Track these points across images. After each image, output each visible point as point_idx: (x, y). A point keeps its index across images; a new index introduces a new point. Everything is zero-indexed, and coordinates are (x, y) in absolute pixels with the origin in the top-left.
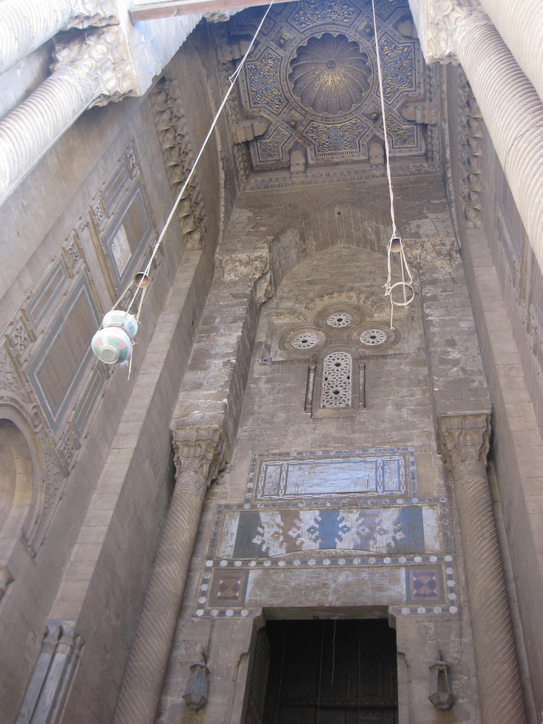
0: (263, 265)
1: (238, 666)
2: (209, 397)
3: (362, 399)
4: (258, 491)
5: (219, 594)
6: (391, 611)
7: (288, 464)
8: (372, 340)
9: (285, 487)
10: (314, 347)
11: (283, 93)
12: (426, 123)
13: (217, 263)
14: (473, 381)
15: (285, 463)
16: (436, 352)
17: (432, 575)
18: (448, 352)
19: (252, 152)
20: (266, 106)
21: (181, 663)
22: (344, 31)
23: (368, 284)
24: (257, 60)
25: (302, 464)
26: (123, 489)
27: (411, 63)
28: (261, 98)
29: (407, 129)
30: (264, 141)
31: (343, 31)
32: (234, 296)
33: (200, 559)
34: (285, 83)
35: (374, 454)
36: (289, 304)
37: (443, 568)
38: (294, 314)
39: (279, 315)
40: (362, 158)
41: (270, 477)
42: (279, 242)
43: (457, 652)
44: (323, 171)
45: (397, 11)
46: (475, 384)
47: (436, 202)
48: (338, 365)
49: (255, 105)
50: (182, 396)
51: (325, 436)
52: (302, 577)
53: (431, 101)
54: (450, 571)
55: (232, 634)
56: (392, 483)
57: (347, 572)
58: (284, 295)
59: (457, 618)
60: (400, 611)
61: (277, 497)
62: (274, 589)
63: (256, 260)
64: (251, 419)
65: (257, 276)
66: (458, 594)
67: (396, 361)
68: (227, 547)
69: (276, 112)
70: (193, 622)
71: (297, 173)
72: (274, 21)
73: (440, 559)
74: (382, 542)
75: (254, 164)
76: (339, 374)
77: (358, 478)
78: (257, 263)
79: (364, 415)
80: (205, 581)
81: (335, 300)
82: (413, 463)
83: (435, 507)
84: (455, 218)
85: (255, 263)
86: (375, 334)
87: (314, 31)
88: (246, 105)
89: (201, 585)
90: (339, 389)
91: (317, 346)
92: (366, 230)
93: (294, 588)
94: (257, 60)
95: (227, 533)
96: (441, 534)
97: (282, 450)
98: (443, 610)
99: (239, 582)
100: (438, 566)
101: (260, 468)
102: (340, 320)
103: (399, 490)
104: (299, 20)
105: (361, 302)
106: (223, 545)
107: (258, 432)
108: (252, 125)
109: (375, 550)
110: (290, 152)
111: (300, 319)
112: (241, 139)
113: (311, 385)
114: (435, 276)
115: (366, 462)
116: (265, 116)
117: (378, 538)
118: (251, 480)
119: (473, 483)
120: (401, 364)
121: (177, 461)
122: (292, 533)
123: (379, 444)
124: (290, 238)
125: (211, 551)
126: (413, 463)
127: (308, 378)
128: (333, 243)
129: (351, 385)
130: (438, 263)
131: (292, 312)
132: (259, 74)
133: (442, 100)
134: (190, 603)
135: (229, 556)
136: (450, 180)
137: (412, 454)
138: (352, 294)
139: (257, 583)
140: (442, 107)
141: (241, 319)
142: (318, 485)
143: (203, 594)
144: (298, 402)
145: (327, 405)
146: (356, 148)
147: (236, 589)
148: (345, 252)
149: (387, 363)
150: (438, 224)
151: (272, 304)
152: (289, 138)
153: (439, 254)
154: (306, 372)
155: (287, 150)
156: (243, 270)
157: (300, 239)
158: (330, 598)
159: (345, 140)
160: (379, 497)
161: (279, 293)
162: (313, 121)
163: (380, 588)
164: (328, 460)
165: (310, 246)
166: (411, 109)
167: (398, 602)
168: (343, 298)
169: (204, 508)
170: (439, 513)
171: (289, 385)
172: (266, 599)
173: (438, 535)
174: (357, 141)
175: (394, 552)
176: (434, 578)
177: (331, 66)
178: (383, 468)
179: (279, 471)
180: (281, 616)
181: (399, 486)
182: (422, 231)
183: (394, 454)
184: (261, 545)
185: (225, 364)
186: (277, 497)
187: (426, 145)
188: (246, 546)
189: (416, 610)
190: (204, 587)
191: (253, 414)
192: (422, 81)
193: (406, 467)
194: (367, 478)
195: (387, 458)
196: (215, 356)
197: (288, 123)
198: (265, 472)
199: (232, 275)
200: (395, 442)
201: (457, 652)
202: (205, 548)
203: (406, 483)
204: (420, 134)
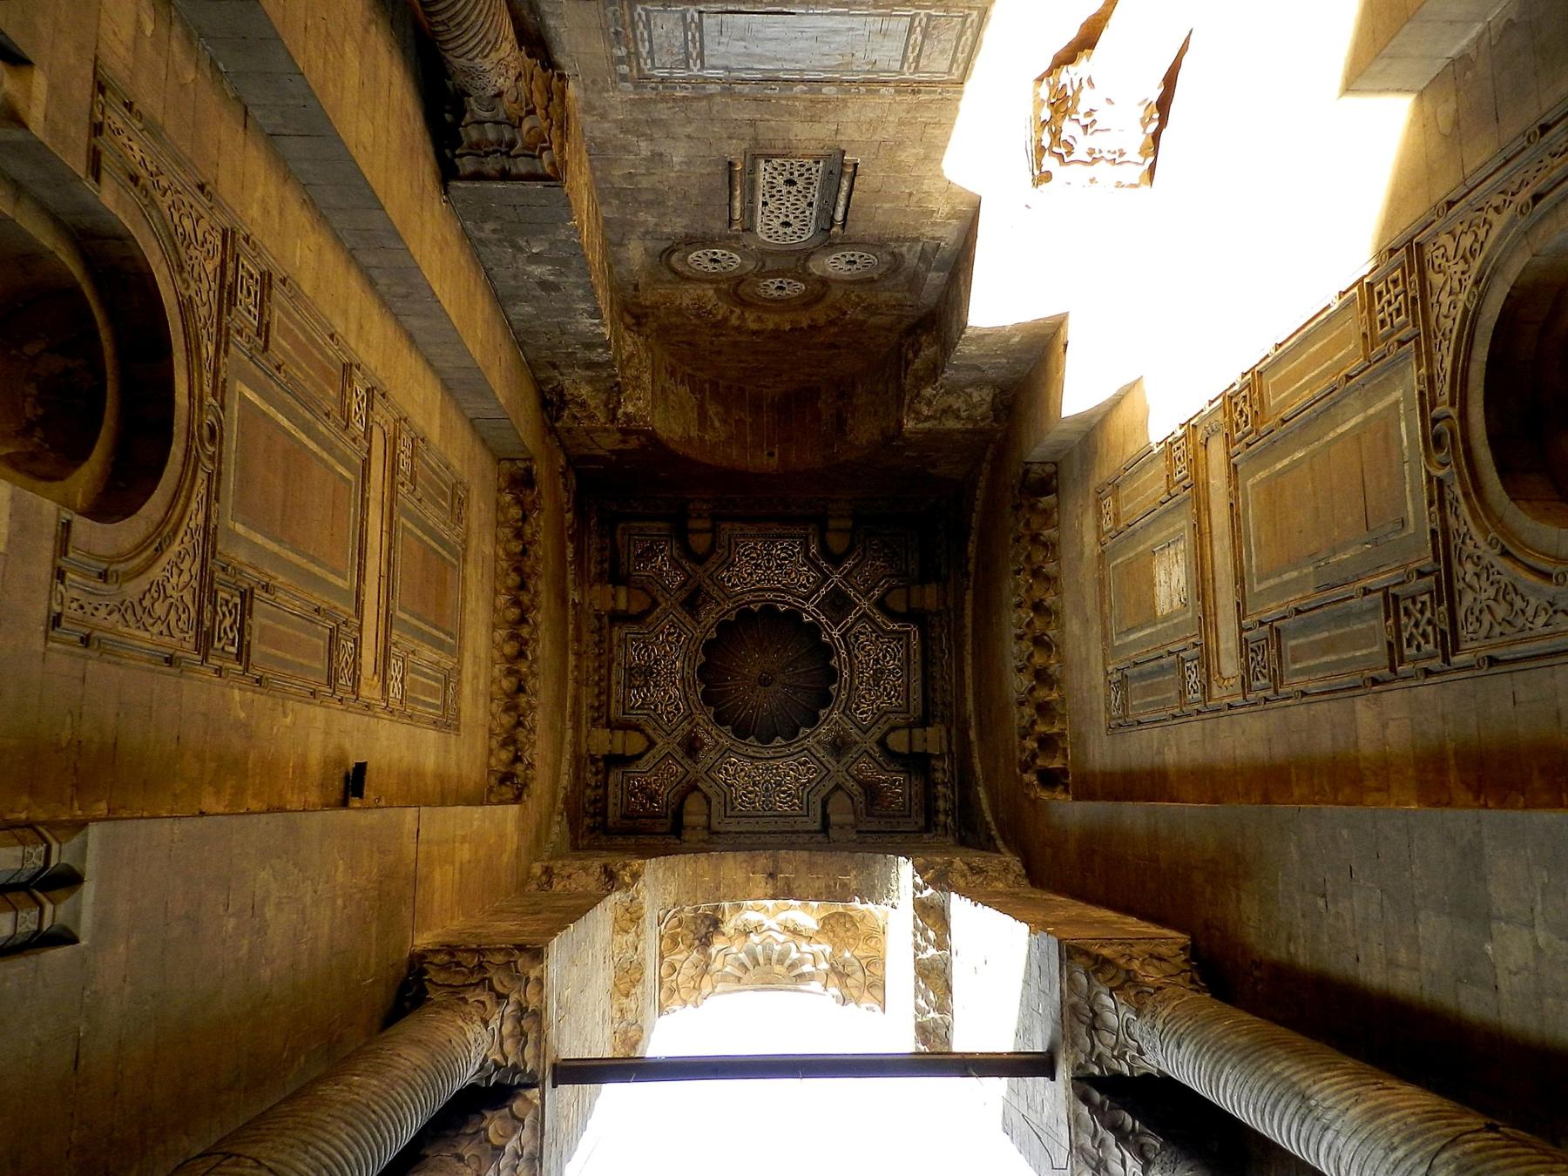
7: (900, 72)
8: (719, 256)
9: (911, 30)
15: (907, 76)
25: (869, 72)
35: (706, 80)
38: (870, 305)
41: (943, 52)
46: (489, 226)
48: (786, 224)
51: (813, 119)
61: (932, 12)
78: (925, 411)
79: (734, 150)
81: (787, 316)
82: (621, 60)
86: (710, 266)
90: (785, 189)
92: (724, 422)
103: (647, 12)
105: (738, 311)
113: (842, 202)
115: (726, 68)
123: (698, 99)
126: (621, 60)
137: (624, 78)
138: (754, 326)
142: (835, 32)
151: (906, 322)
153: (583, 405)
154: (849, 223)
156: (958, 403)
178: (688, 55)
179: (923, 62)
181: (648, 20)
182: (618, 436)
183: (663, 80)
193: (637, 54)
194: (723, 40)
200: (663, 100)
203: (634, 25)
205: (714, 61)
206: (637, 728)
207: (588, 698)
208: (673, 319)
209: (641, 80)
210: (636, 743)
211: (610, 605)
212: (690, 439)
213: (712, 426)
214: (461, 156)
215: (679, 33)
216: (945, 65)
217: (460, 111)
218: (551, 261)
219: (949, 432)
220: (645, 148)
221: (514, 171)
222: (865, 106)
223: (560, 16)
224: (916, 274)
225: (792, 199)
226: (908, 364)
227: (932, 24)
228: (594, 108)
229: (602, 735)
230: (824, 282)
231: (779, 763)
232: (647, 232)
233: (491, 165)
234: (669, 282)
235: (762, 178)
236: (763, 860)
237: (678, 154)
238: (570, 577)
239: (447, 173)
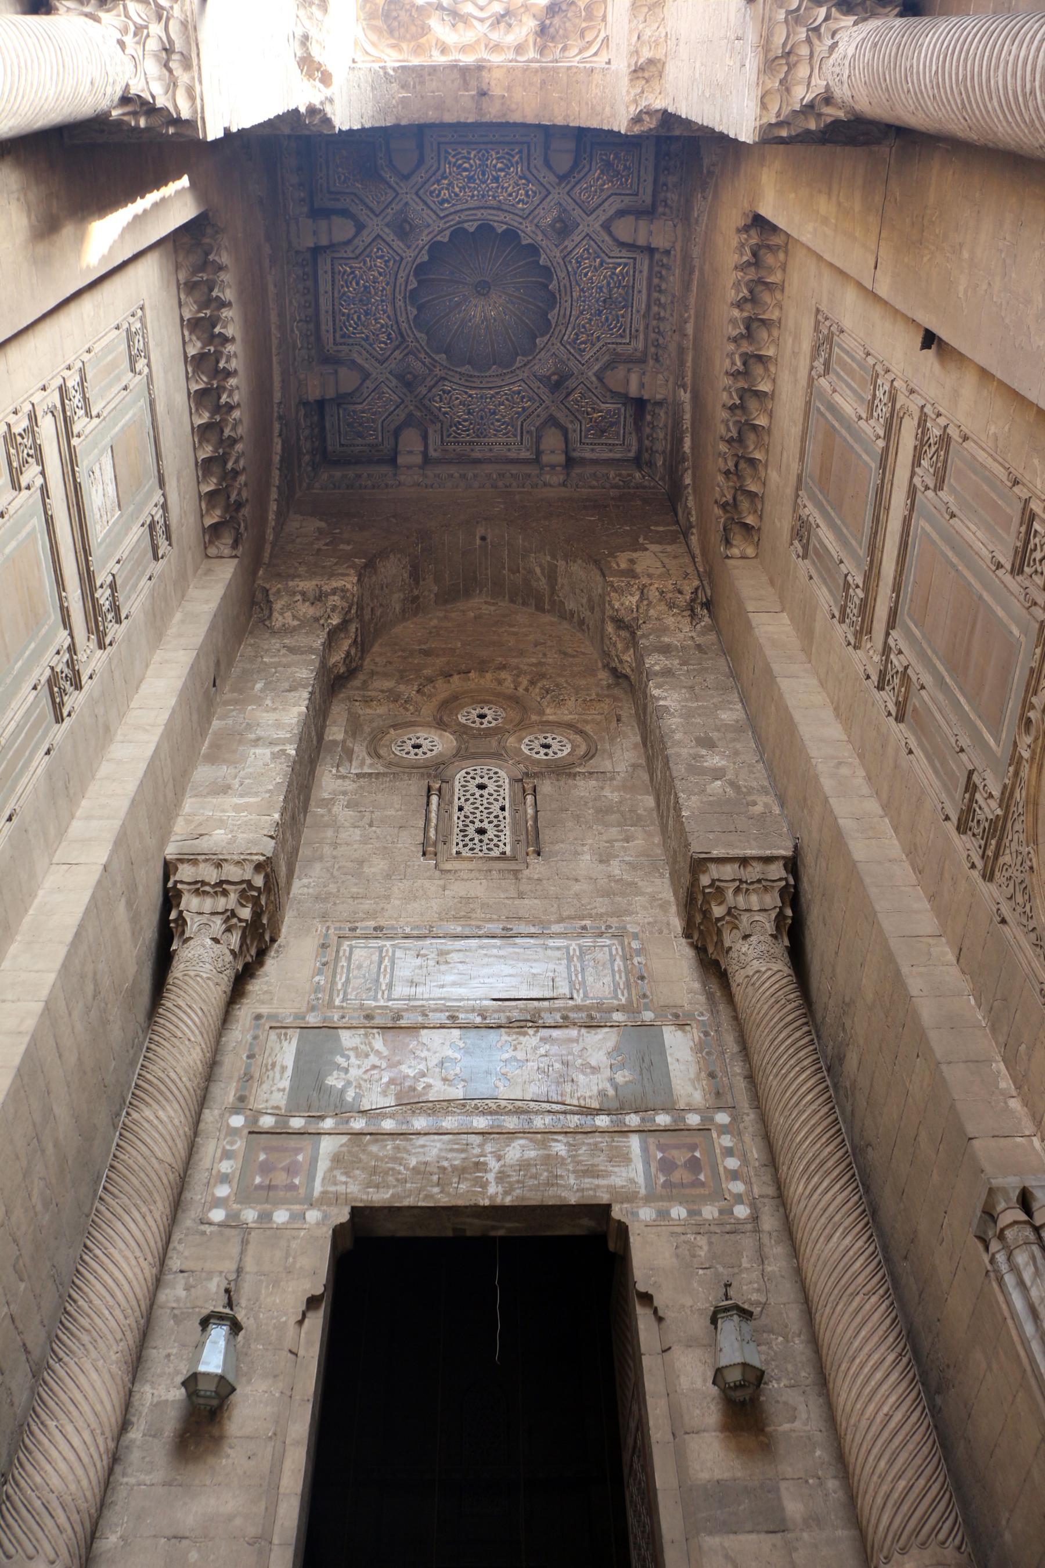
0: (346, 605)
1: (300, 1323)
2: (245, 807)
3: (533, 841)
4: (335, 993)
5: (258, 1180)
6: (616, 1213)
8: (543, 751)
9: (390, 986)
10: (436, 756)
13: (259, 596)
14: (755, 804)
15: (388, 943)
16: (679, 755)
17: (693, 1147)
18: (703, 756)
19: (328, 425)
21: (175, 1316)
23: (534, 660)
24: (357, 258)
26: (77, 935)
27: (627, 293)
29: (609, 412)
30: (352, 407)
31: (514, 222)
32: (291, 650)
33: (216, 1112)
34: (401, 303)
36: (388, 684)
37: (715, 1135)
39: (367, 701)
40: (525, 454)
41: (359, 967)
42: (375, 573)
43: (758, 1290)
44: (453, 470)
45: (611, 200)
46: (758, 809)
47: (661, 529)
48: (482, 787)
50: (189, 804)
51: (467, 900)
52: (433, 1149)
53: (657, 360)
54: (727, 1141)
55: (287, 1258)
56: (601, 985)
57: (522, 1142)
58: (379, 669)
59: (749, 1227)
60: (635, 1214)
62: (374, 1171)
63: (334, 594)
64: (318, 866)
65: (335, 621)
66: (748, 1183)
67: (593, 783)
68: (275, 1091)
70: (204, 1233)
71: (409, 467)
73: (707, 1119)
74: (588, 1088)
75: (330, 448)
76: (478, 814)
77: (534, 975)
78: (335, 600)
79: (537, 868)
80: (227, 1155)
81: (472, 685)
83: (688, 1028)
84: (697, 552)
85: (331, 598)
86: (549, 741)
87: (463, 216)
88: (328, 338)
89: (221, 1160)
90: (485, 825)
91: (441, 754)
92: (531, 572)
93: (415, 1170)
94: (357, 258)
95: (274, 1065)
96: (703, 1075)
97: (382, 922)
98: (721, 1212)
99: (300, 1158)
100: (703, 1130)
101: (338, 951)
102: (482, 716)
103: (616, 997)
104: (438, 196)
105: (521, 690)
106: (265, 1087)
107: (332, 888)
108: (336, 372)
109: (575, 1102)
110: (397, 433)
111: (407, 710)
112: (314, 393)
113: (433, 815)
114: (666, 639)
116: (359, 361)
117: (581, 1078)
118: (319, 972)
119: (769, 973)
120: (602, 788)
121: (175, 921)
122: (409, 1069)
124: (392, 569)
125: (242, 1099)
127: (428, 804)
128: (468, 594)
129: (508, 820)
130: (670, 621)
131: (394, 697)
132: (358, 284)
133: (681, 351)
134: (196, 1195)
135: (278, 1108)
136: (690, 490)
137: (635, 936)
138: (504, 675)
139: (337, 1160)
140: (682, 363)
141: (305, 687)
142: (454, 984)
143: (224, 1179)
144: (409, 841)
145: (466, 853)
146: (515, 436)
147: (291, 1170)
148: (487, 610)
149: (576, 786)
150: (666, 561)
151: (357, 683)
153: (671, 606)
154: (424, 793)
155: (393, 427)
156: (307, 610)
157: (411, 576)
158: (492, 1189)
159: (498, 420)
160: (578, 1008)
161: (367, 664)
162: (445, 379)
163: (591, 1172)
164: (473, 942)
165: (426, 593)
166: (621, 371)
167: (630, 1197)
168: (488, 680)
169: (226, 1018)
170: (697, 1039)
171: (391, 812)
172: (359, 1190)
173: (698, 1078)
175: (616, 1106)
176: (697, 1154)
177: (482, 289)
178: (581, 958)
179: (375, 958)
180: (387, 1228)
181: (615, 991)
182: (639, 569)
183: (601, 935)
184: (343, 1091)
185: (275, 756)
186: (374, 1004)
187: (640, 441)
188: (312, 1091)
189: (668, 1213)
190: (226, 1167)
191: (321, 858)
192: (642, 328)
193: (625, 959)
194: (551, 974)
195: (587, 942)
196: (257, 742)
197: (401, 377)
198: (349, 959)
199: (288, 614)
200: (601, 915)
201: (758, 1290)
202: (226, 1092)
203: (628, 984)
204: (630, 421)
205: (558, 954)
206: (622, 244)
207: (674, 280)
208: (583, 682)
209: (620, 935)
210: (624, 229)
212: (566, 557)
213: (543, 569)
214: (780, 879)
215: (590, 980)
216: (357, 953)
217: (780, 917)
218: (703, 771)
219: (311, 575)
220: (616, 868)
221: (736, 866)
222: (422, 915)
223: (690, 991)
224: (354, 735)
225: (478, 814)
226: (355, 641)
227: (372, 993)
228: (661, 906)
229: (659, 242)
230: (441, 725)
231: (472, 203)
232: (612, 779)
233: (754, 872)
234: (586, 722)
235: (507, 836)
236: (493, 113)
237: (586, 862)
238: (687, 416)
239: (793, 864)
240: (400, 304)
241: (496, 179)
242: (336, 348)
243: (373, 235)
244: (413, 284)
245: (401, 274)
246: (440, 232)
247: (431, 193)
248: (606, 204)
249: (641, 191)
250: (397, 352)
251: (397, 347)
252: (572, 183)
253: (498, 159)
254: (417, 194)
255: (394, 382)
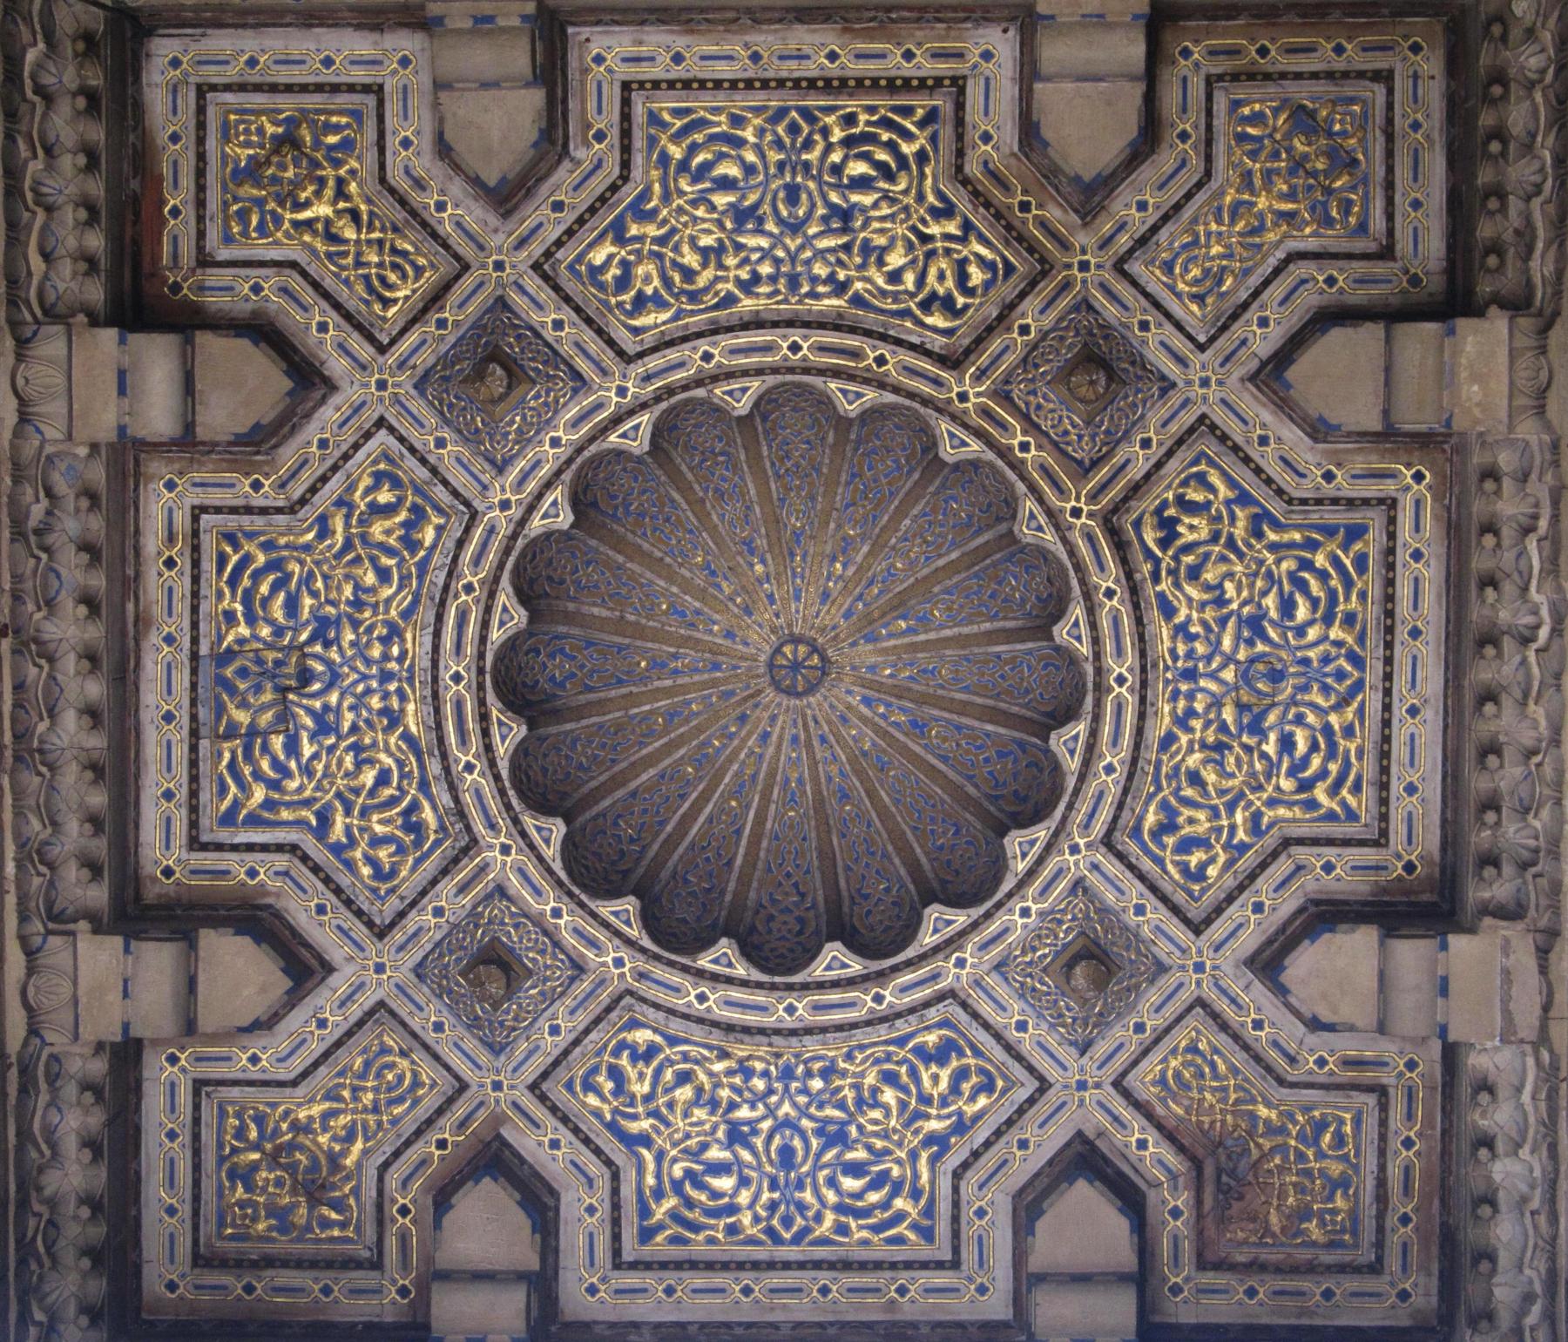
11: (1134, 590)
12: (111, 334)
20: (1275, 507)
22: (659, 972)
24: (1287, 843)
28: (1307, 565)
49: (1356, 517)
69: (1211, 448)
71: (1099, 21)
72: (1126, 1094)
75: (1431, 64)
87: (865, 1002)
88: (1419, 530)
94: (1287, 843)
104: (961, 1075)
112: (1485, 343)
116: (1292, 434)
132: (1287, 743)
152: (1142, 241)
155: (1165, 160)
166: (221, 416)
174: (637, 173)
211: (104, 420)
240: (1121, 666)
241: (737, 1136)
242: (1389, 488)
243: (1218, 930)
244: (1066, 742)
245: (1112, 784)
246: (953, 942)
247: (988, 1087)
248: (315, 1048)
249: (184, 1096)
250: (1136, 471)
251: (1135, 489)
252: (445, 1129)
253: (733, 1209)
254: (1044, 1085)
255: (1156, 344)
